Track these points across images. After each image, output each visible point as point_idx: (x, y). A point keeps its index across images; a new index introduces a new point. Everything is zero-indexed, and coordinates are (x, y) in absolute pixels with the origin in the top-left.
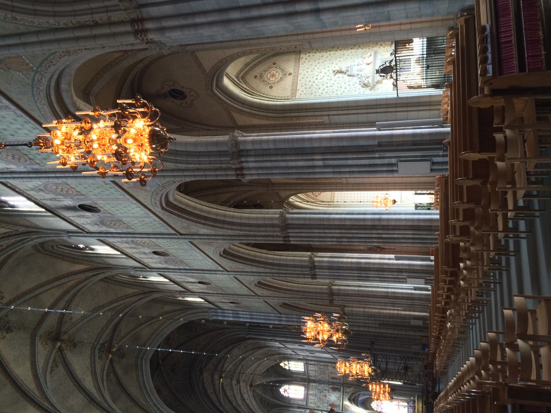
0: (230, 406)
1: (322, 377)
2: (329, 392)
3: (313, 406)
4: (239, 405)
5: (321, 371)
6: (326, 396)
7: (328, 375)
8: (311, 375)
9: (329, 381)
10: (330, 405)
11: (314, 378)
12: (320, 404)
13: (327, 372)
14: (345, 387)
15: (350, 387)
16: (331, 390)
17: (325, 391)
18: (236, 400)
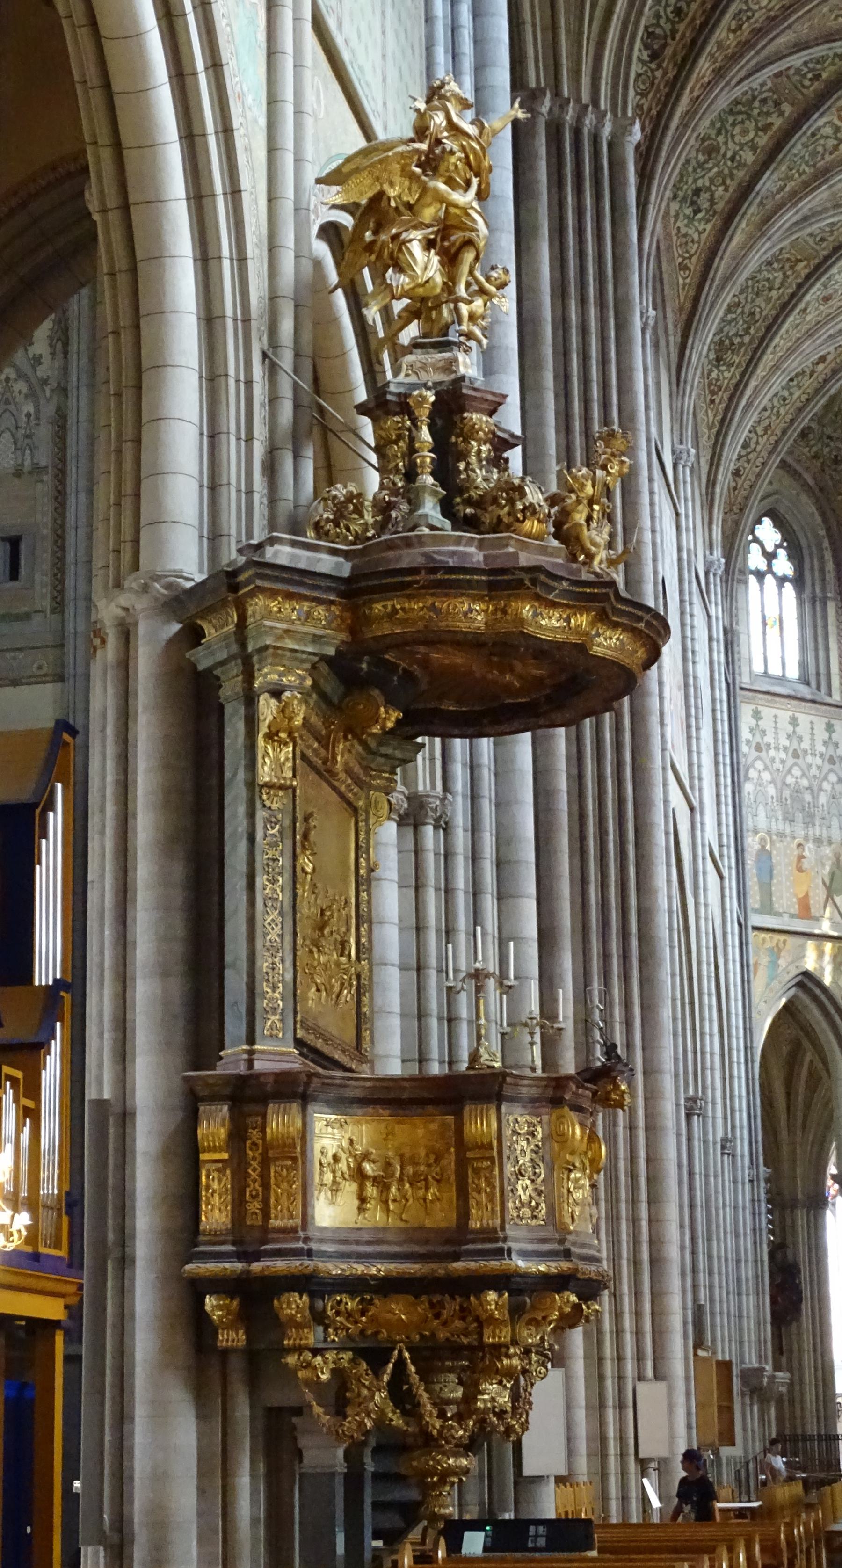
0: (749, 157)
4: (767, 220)
18: (795, 197)
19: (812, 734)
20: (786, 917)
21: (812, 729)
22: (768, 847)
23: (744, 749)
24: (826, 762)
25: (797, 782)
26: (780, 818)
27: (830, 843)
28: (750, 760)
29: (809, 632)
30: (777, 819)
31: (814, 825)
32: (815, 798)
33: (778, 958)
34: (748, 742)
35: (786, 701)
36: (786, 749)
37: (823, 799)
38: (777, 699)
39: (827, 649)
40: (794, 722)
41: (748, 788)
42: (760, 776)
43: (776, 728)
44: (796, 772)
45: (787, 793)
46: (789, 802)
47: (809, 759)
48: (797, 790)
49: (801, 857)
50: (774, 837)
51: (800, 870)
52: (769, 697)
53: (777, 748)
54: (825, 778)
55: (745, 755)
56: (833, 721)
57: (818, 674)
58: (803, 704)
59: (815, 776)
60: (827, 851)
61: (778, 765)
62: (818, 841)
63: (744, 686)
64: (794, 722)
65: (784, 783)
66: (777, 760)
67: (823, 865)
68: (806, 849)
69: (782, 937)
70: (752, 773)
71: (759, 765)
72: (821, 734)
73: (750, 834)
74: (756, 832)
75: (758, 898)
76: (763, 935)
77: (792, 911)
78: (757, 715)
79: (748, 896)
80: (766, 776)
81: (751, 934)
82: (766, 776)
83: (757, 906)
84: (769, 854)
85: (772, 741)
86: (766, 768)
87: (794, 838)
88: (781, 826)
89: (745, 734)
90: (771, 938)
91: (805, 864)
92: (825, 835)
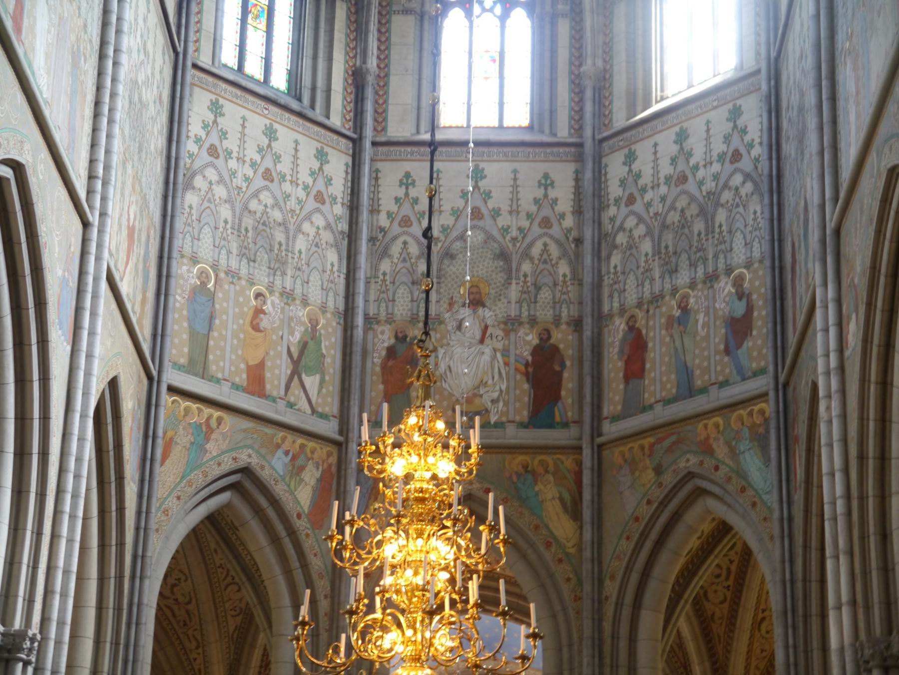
1: (632, 246)
2: (511, 324)
3: (387, 204)
5: (684, 224)
6: (476, 302)
7: (657, 299)
8: (643, 150)
9: (601, 319)
10: (401, 338)
11: (614, 190)
12: (405, 257)
13: (683, 278)
14: (568, 462)
15: (575, 514)
16: (532, 338)
17: (514, 292)
19: (295, 157)
20: (226, 387)
21: (296, 150)
22: (210, 285)
23: (190, 146)
24: (311, 198)
25: (265, 212)
26: (235, 251)
27: (305, 303)
28: (197, 165)
29: (308, 33)
30: (229, 252)
31: (284, 274)
32: (290, 239)
33: (207, 439)
34: (198, 140)
35: (263, 104)
36: (253, 164)
37: (301, 244)
38: (251, 98)
39: (330, 59)
40: (270, 133)
41: (191, 199)
42: (210, 189)
43: (243, 134)
44: (266, 197)
45: (248, 222)
46: (250, 234)
47: (287, 187)
48: (263, 224)
49: (258, 312)
50: (222, 275)
51: (256, 328)
52: (239, 92)
53: (241, 160)
54: (308, 218)
55: (191, 155)
56: (326, 149)
57: (314, 89)
58: (287, 115)
59: (293, 211)
60: (302, 313)
61: (239, 181)
62: (288, 296)
63: (200, 64)
64: (270, 133)
65: (246, 208)
66: (240, 175)
67: (292, 332)
68: (269, 302)
69: (216, 414)
70: (198, 181)
71: (211, 174)
72: (308, 161)
73: (185, 261)
74: (194, 260)
75: (186, 350)
76: (185, 404)
77: (237, 380)
78: (216, 108)
79: (168, 340)
80: (220, 192)
81: (167, 399)
82: (220, 192)
83: (183, 361)
84: (212, 296)
85: (235, 149)
86: (221, 181)
87: (253, 284)
88: (234, 264)
89: (194, 125)
90: (200, 410)
91: (265, 323)
92: (298, 291)
